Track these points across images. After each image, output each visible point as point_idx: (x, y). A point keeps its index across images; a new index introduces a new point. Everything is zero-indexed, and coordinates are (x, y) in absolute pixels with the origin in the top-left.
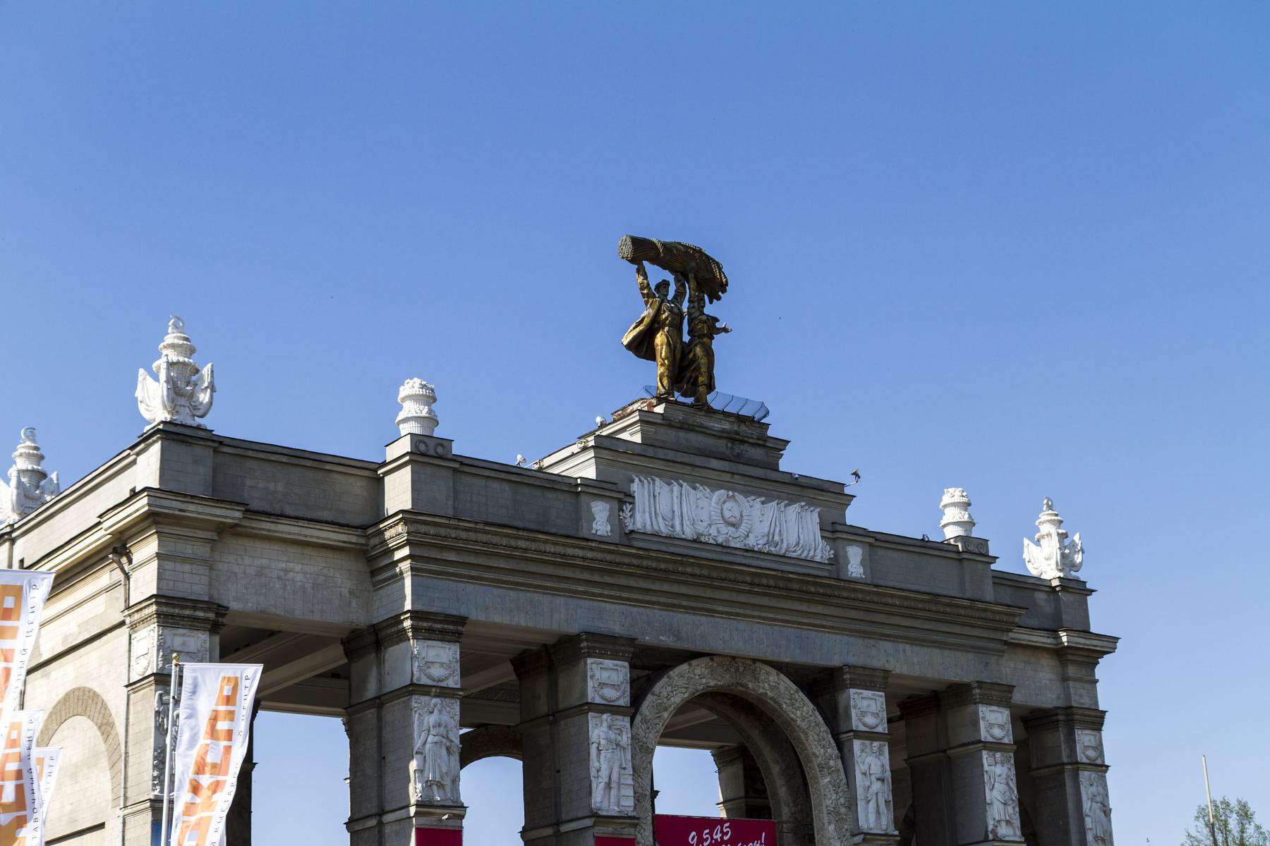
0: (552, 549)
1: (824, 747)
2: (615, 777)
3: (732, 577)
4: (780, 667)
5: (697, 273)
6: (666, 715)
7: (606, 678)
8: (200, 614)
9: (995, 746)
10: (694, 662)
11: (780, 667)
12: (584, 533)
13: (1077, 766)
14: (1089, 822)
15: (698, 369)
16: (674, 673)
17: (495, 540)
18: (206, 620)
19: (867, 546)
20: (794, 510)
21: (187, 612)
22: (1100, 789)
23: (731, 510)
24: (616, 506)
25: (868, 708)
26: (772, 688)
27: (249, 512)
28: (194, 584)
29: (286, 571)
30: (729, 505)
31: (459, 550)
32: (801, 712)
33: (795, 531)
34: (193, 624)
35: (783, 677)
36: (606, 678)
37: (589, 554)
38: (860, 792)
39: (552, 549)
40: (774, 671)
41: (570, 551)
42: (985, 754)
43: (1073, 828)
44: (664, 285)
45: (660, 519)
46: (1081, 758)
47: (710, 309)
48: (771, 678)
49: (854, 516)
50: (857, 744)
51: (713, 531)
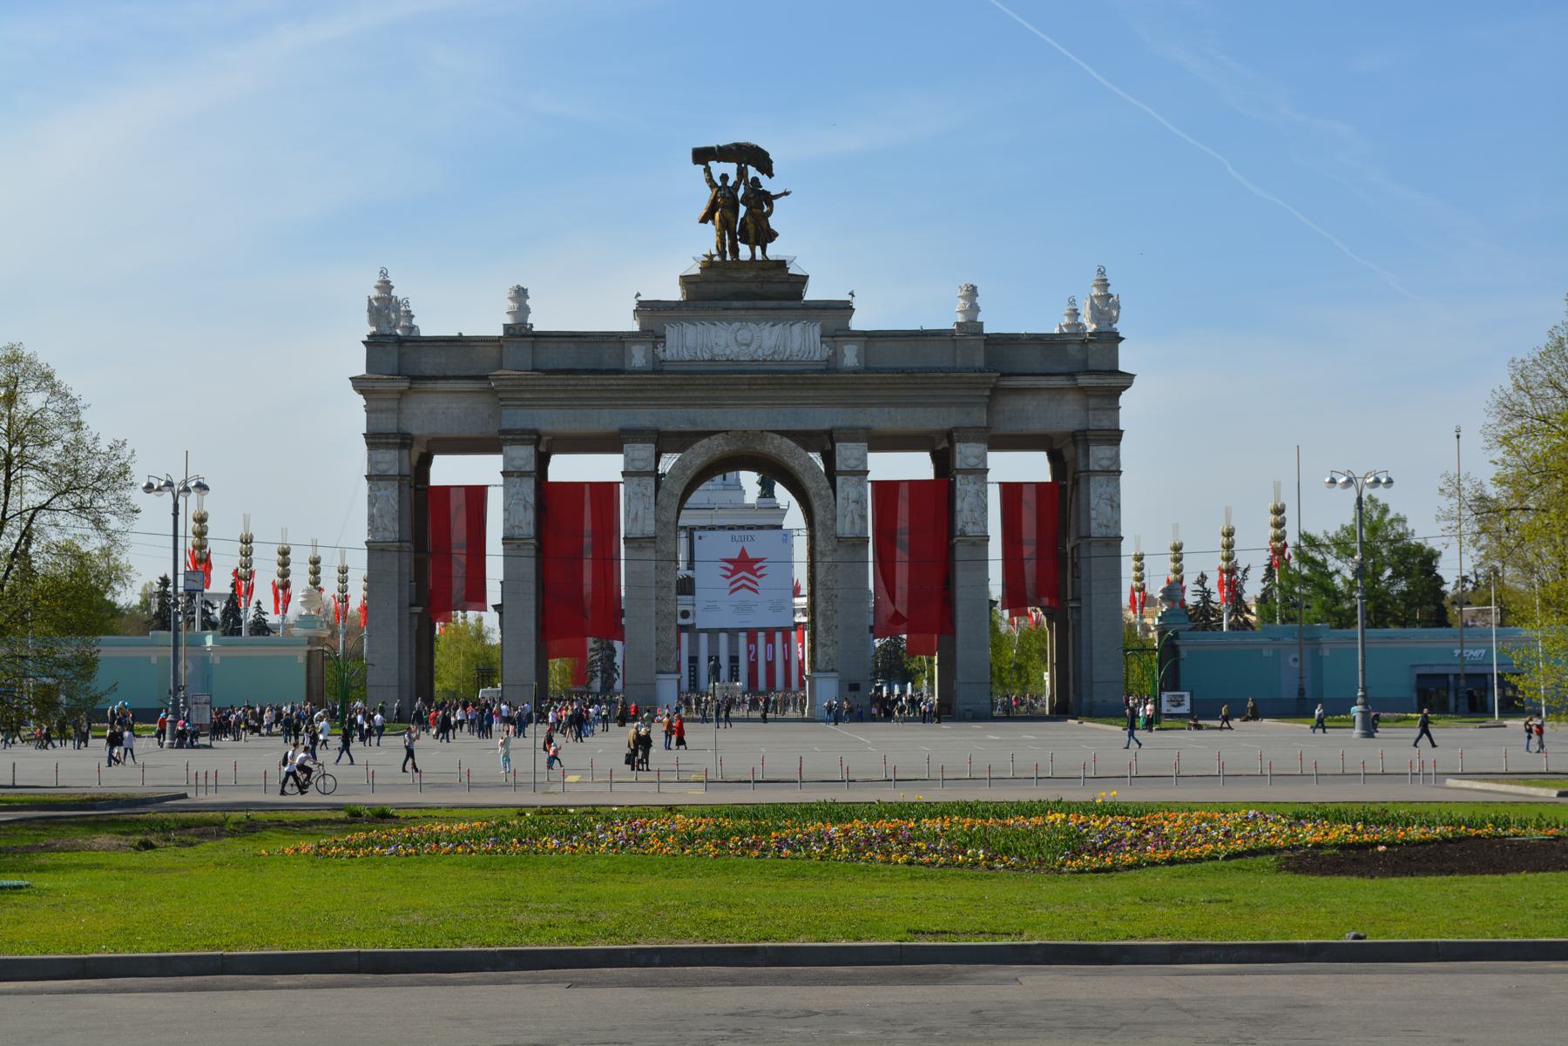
4: (783, 433)
11: (783, 433)
12: (627, 367)
13: (1090, 473)
14: (1093, 514)
20: (797, 328)
23: (744, 335)
24: (650, 346)
27: (414, 378)
28: (388, 424)
31: (531, 391)
34: (388, 446)
42: (959, 477)
44: (724, 177)
47: (764, 180)
49: (858, 323)
50: (839, 480)
51: (728, 352)
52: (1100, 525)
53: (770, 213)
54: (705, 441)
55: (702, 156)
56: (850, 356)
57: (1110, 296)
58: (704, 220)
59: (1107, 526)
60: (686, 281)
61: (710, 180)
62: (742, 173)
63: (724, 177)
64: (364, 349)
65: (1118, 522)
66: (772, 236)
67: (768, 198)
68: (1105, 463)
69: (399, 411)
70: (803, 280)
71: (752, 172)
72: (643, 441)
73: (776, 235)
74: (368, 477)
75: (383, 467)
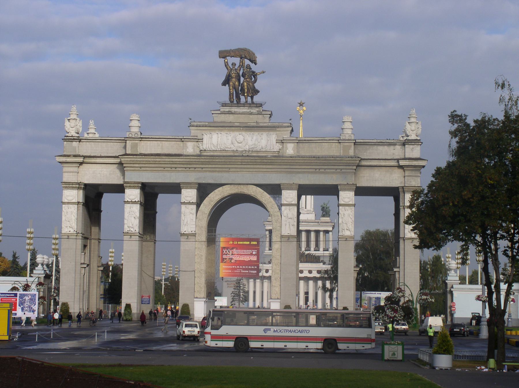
0: (168, 160)
2: (188, 223)
3: (234, 161)
6: (212, 203)
7: (189, 194)
8: (74, 186)
17: (149, 160)
18: (76, 187)
19: (296, 144)
21: (71, 186)
29: (101, 171)
34: (73, 188)
37: (181, 160)
38: (283, 223)
39: (168, 160)
40: (255, 187)
41: (174, 160)
50: (283, 208)
53: (255, 81)
55: (223, 55)
56: (290, 150)
58: (224, 84)
61: (226, 64)
66: (257, 92)
67: (254, 74)
71: (247, 62)
72: (191, 188)
73: (258, 92)
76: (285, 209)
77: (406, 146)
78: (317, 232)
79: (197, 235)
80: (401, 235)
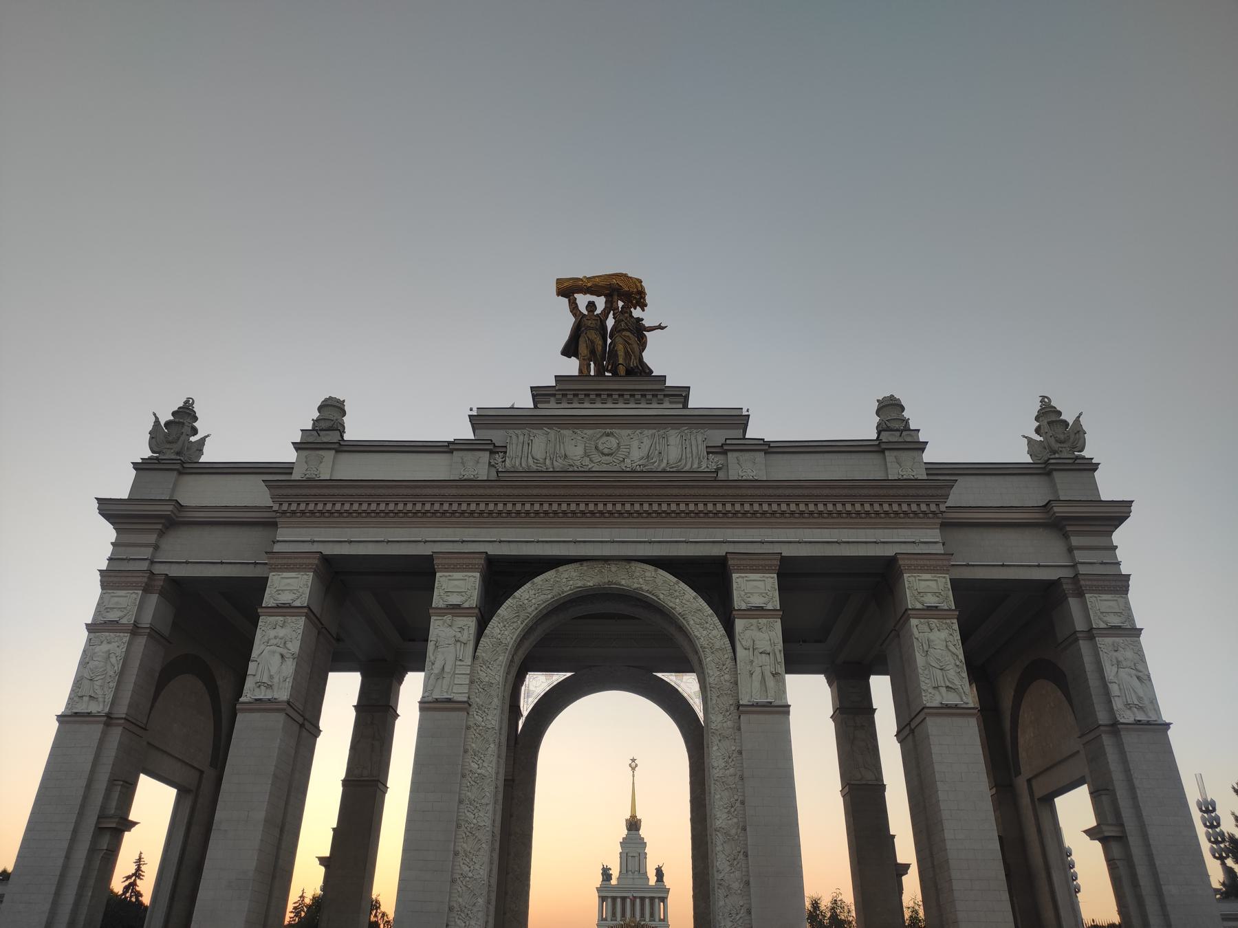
1: (706, 629)
2: (447, 669)
5: (625, 293)
7: (458, 587)
9: (931, 612)
10: (560, 569)
13: (1091, 634)
14: (1114, 689)
15: (617, 355)
16: (538, 580)
22: (1129, 654)
25: (755, 589)
26: (647, 582)
30: (605, 439)
32: (684, 601)
33: (678, 452)
35: (661, 572)
36: (458, 587)
40: (651, 568)
42: (914, 622)
43: (1098, 701)
45: (530, 460)
46: (1097, 623)
47: (637, 313)
48: (648, 574)
51: (586, 461)
52: (1128, 706)
54: (550, 574)
55: (567, 289)
57: (1066, 423)
59: (1141, 708)
60: (539, 394)
61: (574, 307)
62: (610, 306)
63: (591, 306)
64: (133, 473)
65: (1153, 701)
68: (1115, 621)
69: (156, 547)
70: (682, 394)
74: (90, 628)
75: (113, 616)
76: (747, 629)
77: (1055, 474)
78: (652, 899)
79: (473, 711)
80: (1102, 717)
